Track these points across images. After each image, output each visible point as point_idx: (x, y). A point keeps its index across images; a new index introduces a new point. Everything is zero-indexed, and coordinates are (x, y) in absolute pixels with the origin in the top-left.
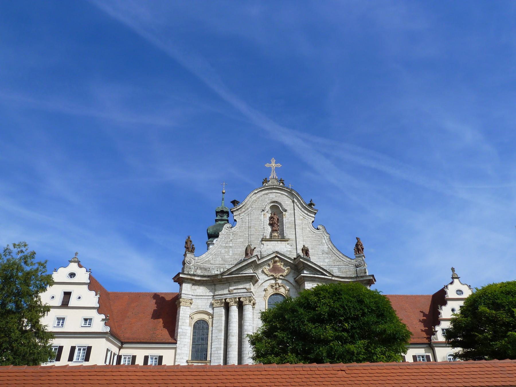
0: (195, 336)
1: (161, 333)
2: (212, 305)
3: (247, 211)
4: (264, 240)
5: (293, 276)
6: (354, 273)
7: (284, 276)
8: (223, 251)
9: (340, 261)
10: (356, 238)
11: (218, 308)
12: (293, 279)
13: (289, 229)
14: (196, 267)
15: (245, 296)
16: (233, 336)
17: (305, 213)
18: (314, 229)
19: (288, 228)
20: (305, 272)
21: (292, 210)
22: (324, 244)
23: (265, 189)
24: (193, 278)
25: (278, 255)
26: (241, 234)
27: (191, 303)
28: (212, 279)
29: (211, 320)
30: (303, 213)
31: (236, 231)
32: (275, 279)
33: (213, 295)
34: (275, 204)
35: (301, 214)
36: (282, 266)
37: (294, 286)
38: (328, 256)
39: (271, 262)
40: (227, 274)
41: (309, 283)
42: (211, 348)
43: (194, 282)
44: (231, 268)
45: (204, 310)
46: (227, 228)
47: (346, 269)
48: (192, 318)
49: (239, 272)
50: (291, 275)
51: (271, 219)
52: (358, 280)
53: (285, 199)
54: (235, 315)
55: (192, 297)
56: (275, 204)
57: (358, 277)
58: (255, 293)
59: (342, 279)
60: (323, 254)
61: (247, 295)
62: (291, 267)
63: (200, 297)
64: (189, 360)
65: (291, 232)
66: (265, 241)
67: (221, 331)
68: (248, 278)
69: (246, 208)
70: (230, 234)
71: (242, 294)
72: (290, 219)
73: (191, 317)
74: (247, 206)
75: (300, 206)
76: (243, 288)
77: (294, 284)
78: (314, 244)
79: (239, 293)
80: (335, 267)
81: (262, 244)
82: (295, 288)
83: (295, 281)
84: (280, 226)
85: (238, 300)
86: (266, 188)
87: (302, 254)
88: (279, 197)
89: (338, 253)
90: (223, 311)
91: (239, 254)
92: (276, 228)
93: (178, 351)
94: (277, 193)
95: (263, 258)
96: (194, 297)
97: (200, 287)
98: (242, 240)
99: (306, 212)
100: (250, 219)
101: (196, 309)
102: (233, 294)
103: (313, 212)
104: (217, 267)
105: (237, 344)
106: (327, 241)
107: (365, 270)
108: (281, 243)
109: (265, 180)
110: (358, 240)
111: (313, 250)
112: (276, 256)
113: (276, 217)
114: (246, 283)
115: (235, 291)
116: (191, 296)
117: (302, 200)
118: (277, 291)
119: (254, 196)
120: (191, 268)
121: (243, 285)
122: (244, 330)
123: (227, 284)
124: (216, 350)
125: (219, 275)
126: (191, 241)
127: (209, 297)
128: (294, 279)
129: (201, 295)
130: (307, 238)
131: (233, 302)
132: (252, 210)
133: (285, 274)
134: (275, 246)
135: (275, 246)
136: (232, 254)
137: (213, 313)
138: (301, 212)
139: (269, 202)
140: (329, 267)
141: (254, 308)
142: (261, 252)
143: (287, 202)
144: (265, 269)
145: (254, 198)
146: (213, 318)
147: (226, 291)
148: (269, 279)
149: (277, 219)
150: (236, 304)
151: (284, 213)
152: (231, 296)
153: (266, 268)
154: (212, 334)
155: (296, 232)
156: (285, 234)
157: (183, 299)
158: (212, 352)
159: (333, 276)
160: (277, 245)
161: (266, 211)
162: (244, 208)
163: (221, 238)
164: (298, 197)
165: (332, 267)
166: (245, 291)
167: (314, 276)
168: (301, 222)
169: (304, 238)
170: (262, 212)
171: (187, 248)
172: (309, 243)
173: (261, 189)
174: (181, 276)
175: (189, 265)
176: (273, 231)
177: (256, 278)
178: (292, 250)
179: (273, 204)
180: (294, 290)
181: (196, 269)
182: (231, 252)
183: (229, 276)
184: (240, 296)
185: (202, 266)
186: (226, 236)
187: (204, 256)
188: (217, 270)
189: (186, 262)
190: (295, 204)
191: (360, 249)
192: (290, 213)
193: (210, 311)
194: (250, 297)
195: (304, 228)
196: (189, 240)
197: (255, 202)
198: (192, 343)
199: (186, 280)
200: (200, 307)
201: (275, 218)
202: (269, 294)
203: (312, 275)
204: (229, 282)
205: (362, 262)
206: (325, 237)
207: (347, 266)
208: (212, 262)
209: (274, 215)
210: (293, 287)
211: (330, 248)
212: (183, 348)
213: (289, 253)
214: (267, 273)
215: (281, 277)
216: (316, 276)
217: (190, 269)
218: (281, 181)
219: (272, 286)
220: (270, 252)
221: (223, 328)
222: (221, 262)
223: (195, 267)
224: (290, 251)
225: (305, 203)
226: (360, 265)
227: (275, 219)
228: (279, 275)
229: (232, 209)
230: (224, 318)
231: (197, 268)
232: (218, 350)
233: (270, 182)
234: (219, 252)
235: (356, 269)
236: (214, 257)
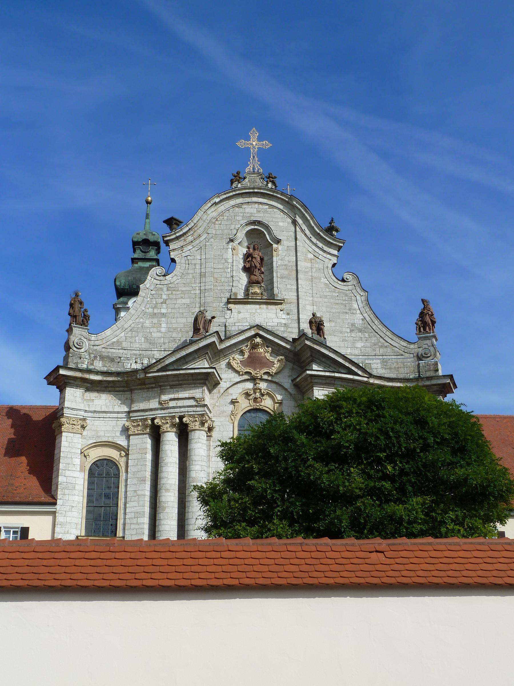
0: (92, 489)
1: (24, 485)
2: (125, 430)
3: (198, 241)
4: (232, 301)
5: (290, 374)
6: (414, 371)
7: (271, 375)
8: (148, 323)
9: (386, 347)
10: (422, 300)
11: (137, 437)
12: (290, 381)
13: (284, 280)
14: (92, 356)
15: (193, 413)
16: (167, 490)
17: (318, 247)
18: (336, 280)
19: (282, 277)
20: (315, 367)
21: (291, 239)
22: (354, 311)
24: (87, 376)
25: (261, 333)
26: (184, 289)
27: (83, 427)
28: (126, 379)
29: (124, 459)
30: (314, 247)
31: (176, 283)
32: (253, 379)
33: (127, 410)
34: (256, 227)
35: (310, 250)
36: (268, 355)
37: (291, 394)
38: (363, 336)
39: (247, 346)
40: (155, 369)
41: (322, 389)
42: (125, 513)
43: (89, 385)
44: (163, 358)
45: (110, 440)
46: (155, 275)
47: (397, 362)
48: (85, 456)
49: (180, 365)
50: (286, 372)
51: (247, 259)
52: (420, 384)
53: (277, 216)
54: (171, 450)
55: (86, 414)
56: (256, 227)
57: (422, 379)
58: (213, 408)
59: (388, 381)
60: (351, 331)
61: (195, 411)
62: (286, 357)
63: (101, 415)
64: (81, 536)
65: (288, 286)
66: (235, 303)
67: (145, 481)
68: (199, 377)
69: (196, 235)
70: (162, 289)
71: (187, 409)
72: (287, 258)
73: (83, 454)
74: (198, 231)
75: (307, 232)
76: (189, 398)
77: (292, 390)
78: (334, 311)
79: (180, 407)
80: (376, 359)
81: (228, 309)
82: (293, 398)
83: (294, 385)
84: (266, 273)
85: (177, 420)
86: (237, 192)
87: (309, 331)
88: (266, 212)
89: (384, 329)
90: (148, 442)
91: (181, 330)
92: (257, 276)
93: (60, 519)
94: (261, 203)
95: (230, 338)
96: (90, 415)
97: (101, 395)
98: (187, 301)
99: (320, 245)
100: (203, 257)
101: (93, 437)
102: (168, 408)
103: (336, 245)
104: (136, 355)
105: (176, 505)
106: (361, 305)
107: (436, 364)
108: (267, 308)
109: (235, 176)
110: (424, 304)
111: (333, 324)
112: (257, 335)
113: (257, 255)
114: (195, 387)
115: (172, 404)
116: (82, 413)
117: (312, 219)
118: (257, 404)
119: (213, 209)
120: (82, 356)
121: (188, 392)
122: (191, 479)
123: (156, 389)
124: (135, 518)
125: (140, 372)
126: (81, 303)
127: (120, 415)
128: (292, 381)
129: (103, 410)
131: (168, 425)
132: (207, 240)
133: (273, 370)
134: (254, 313)
135: (254, 313)
136: (168, 329)
137: (129, 446)
138: (311, 244)
139: (243, 222)
140: (364, 357)
141: (211, 436)
142: (225, 326)
143: (281, 224)
144: (234, 359)
145: (213, 213)
146: (127, 455)
147: (154, 404)
148: (241, 379)
149: (259, 259)
150: (175, 429)
151: (275, 246)
152: (165, 413)
153: (236, 359)
154: (126, 486)
155: (299, 286)
156: (275, 289)
157: (68, 417)
158: (128, 521)
159: (371, 375)
160: (258, 311)
161: (237, 242)
162: (192, 234)
163: (144, 297)
164: (305, 213)
165: (371, 357)
166: (192, 402)
167: (333, 374)
168: (309, 265)
169: (315, 299)
170: (228, 243)
171: (73, 316)
172: (324, 309)
173: (228, 195)
174: (62, 372)
175: (78, 350)
176: (251, 283)
177: (215, 379)
178: (290, 322)
179: (253, 227)
180: (292, 403)
181: (92, 358)
182: (164, 325)
183: (160, 374)
184: (182, 414)
185: (105, 353)
186: (153, 292)
187: (108, 332)
188: (136, 362)
189: (71, 344)
190: (298, 229)
191: (429, 324)
192: (288, 247)
193: (122, 442)
194: (203, 415)
195: (315, 278)
196: (76, 300)
197: (214, 223)
198: (87, 504)
199: (72, 381)
200: (101, 434)
201: (256, 256)
202: (240, 409)
203: (327, 374)
204: (160, 386)
205: (432, 349)
206: (358, 297)
207: (399, 357)
208: (125, 345)
209: (254, 249)
210: (289, 396)
211: (368, 319)
212: (69, 514)
213: (282, 329)
214: (238, 369)
215: (265, 377)
216: (337, 375)
217: (80, 358)
218: (270, 178)
219: (247, 395)
220: (246, 325)
221: (148, 474)
222: (144, 346)
223: (90, 354)
224: (285, 324)
225: (319, 226)
226: (426, 356)
227: (255, 258)
228: (263, 372)
229: (166, 237)
230: (149, 456)
231: (95, 357)
232: (137, 517)
233: (247, 180)
234: (140, 326)
235: (417, 363)
236: (129, 335)
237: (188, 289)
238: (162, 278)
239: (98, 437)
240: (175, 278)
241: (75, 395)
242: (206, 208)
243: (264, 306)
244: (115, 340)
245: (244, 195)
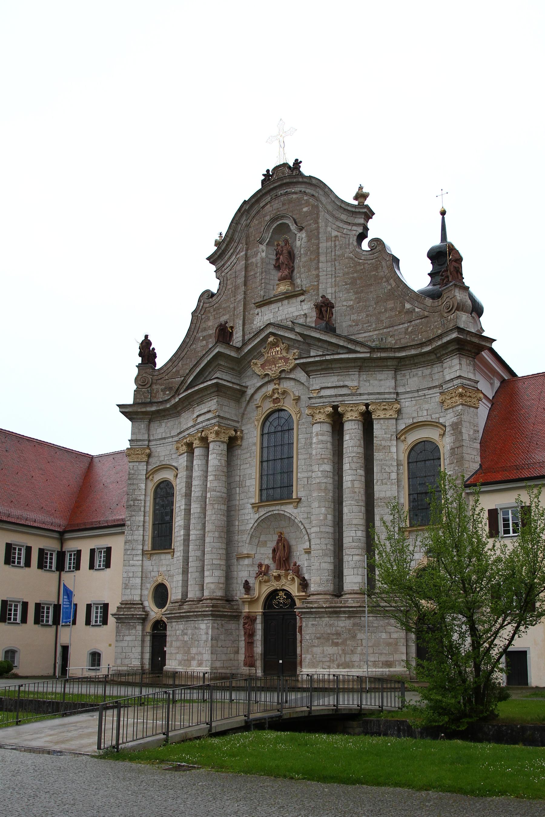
135: (277, 312)
199: (135, 416)
224: (304, 315)
236: (185, 363)
237: (228, 304)
239: (161, 461)
240: (219, 298)
241: (140, 427)
243: (286, 302)
244: (174, 370)
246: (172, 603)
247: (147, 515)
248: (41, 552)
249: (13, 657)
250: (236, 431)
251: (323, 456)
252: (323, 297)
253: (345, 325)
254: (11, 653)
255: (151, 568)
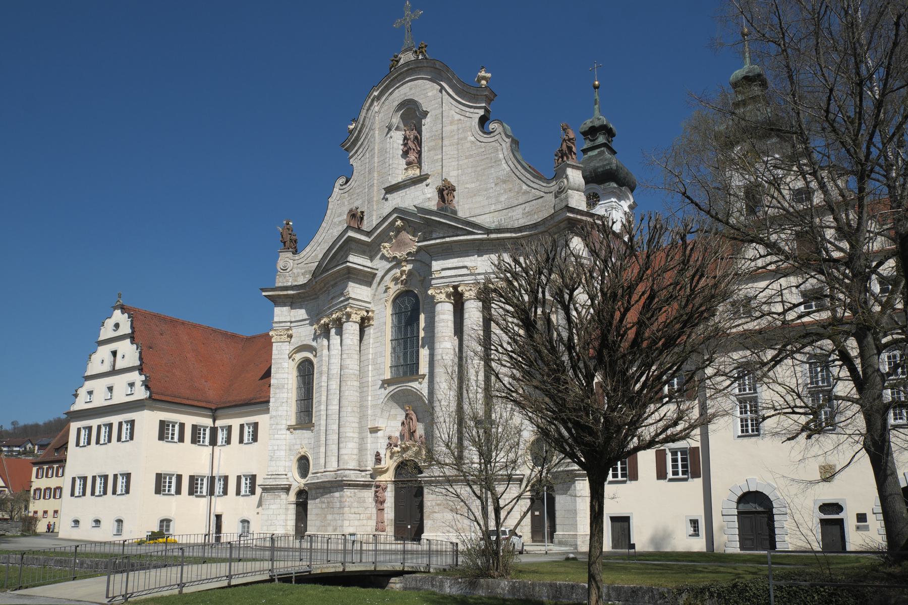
23: (392, 80)
26: (358, 191)
78: (479, 169)
106: (506, 153)
116: (289, 324)
130: (466, 161)
169: (461, 163)
237: (361, 189)
238: (344, 187)
242: (368, 105)
245: (399, 78)
246: (313, 474)
247: (290, 391)
248: (195, 428)
249: (168, 526)
250: (368, 312)
251: (444, 334)
252: (445, 180)
253: (467, 206)
254: (165, 523)
255: (294, 441)
